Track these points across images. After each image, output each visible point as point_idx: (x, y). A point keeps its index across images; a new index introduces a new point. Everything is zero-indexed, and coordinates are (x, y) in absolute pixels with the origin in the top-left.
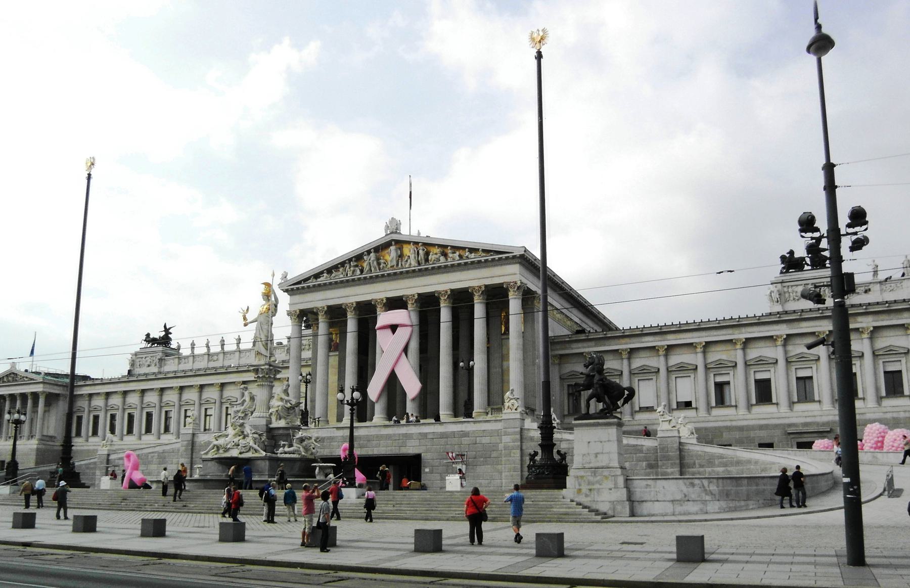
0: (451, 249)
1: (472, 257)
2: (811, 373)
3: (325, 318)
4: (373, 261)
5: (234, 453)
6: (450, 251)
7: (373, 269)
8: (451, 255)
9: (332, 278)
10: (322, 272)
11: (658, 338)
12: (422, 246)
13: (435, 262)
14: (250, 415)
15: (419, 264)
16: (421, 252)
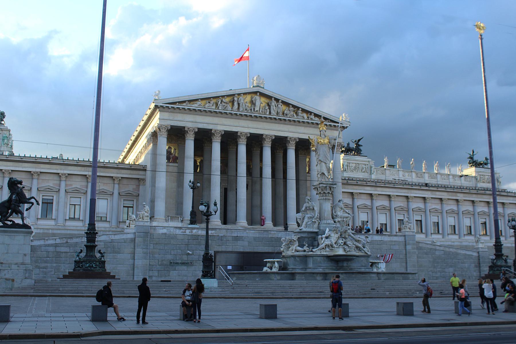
0: (301, 111)
1: (315, 120)
2: (421, 218)
3: (193, 137)
4: (243, 103)
5: (340, 252)
6: (300, 111)
7: (241, 109)
8: (300, 114)
9: (206, 107)
10: (197, 100)
11: (373, 188)
12: (281, 102)
13: (291, 116)
14: (319, 221)
15: (278, 113)
16: (280, 106)
